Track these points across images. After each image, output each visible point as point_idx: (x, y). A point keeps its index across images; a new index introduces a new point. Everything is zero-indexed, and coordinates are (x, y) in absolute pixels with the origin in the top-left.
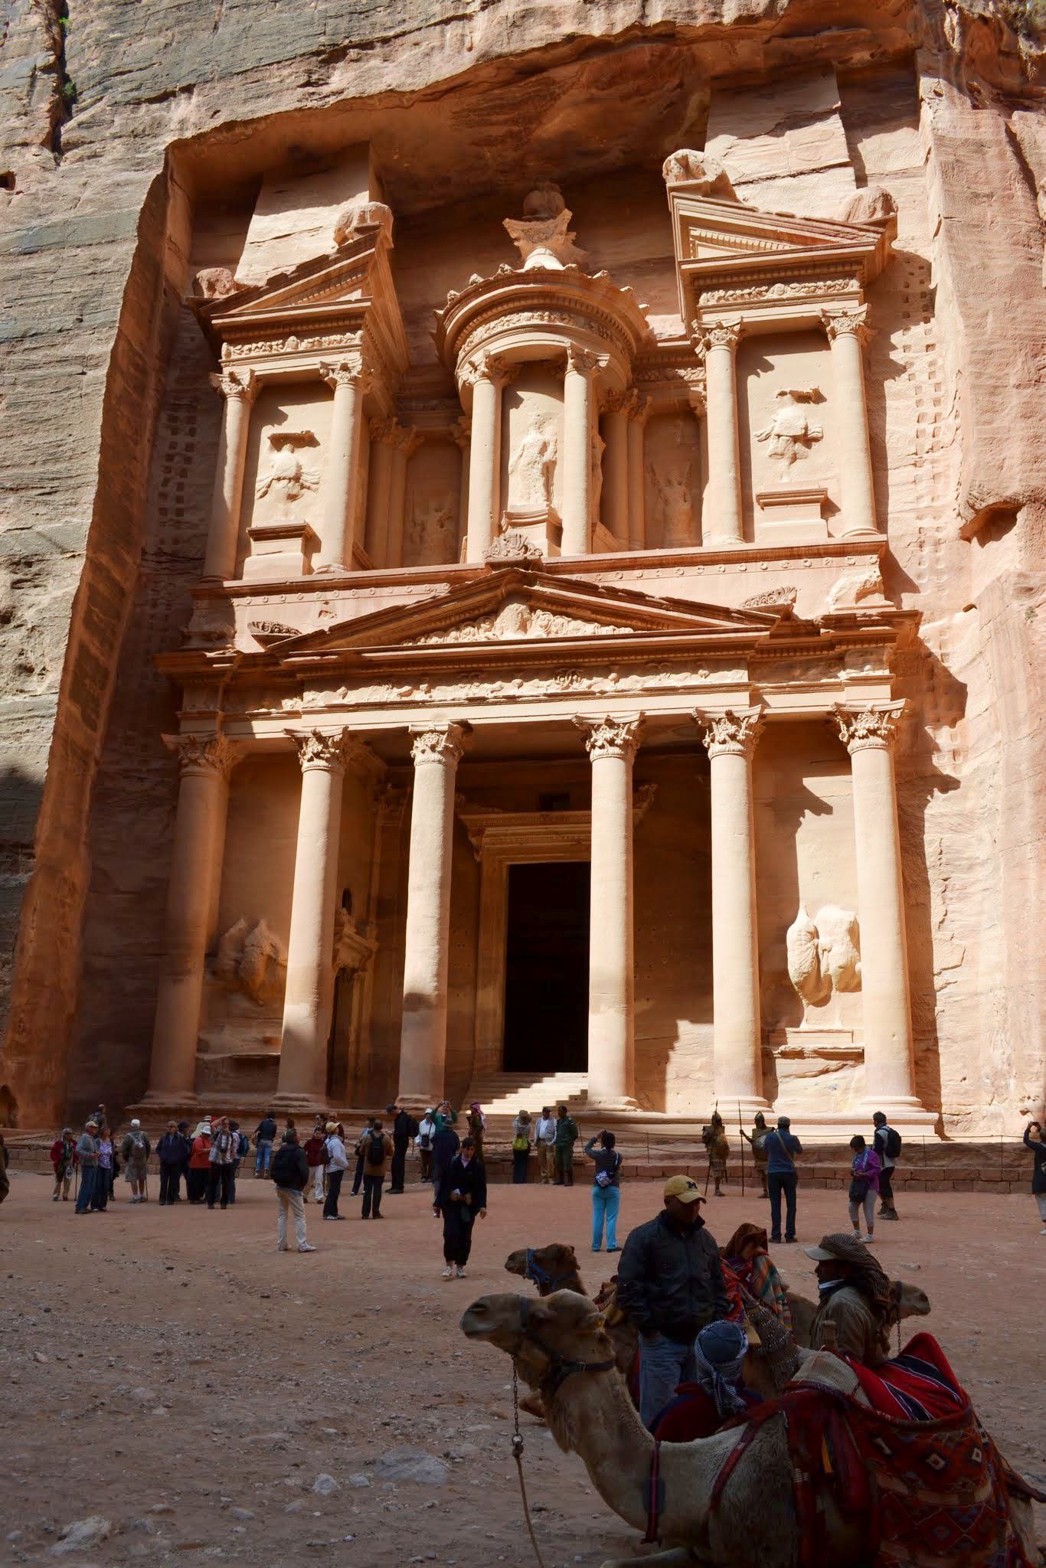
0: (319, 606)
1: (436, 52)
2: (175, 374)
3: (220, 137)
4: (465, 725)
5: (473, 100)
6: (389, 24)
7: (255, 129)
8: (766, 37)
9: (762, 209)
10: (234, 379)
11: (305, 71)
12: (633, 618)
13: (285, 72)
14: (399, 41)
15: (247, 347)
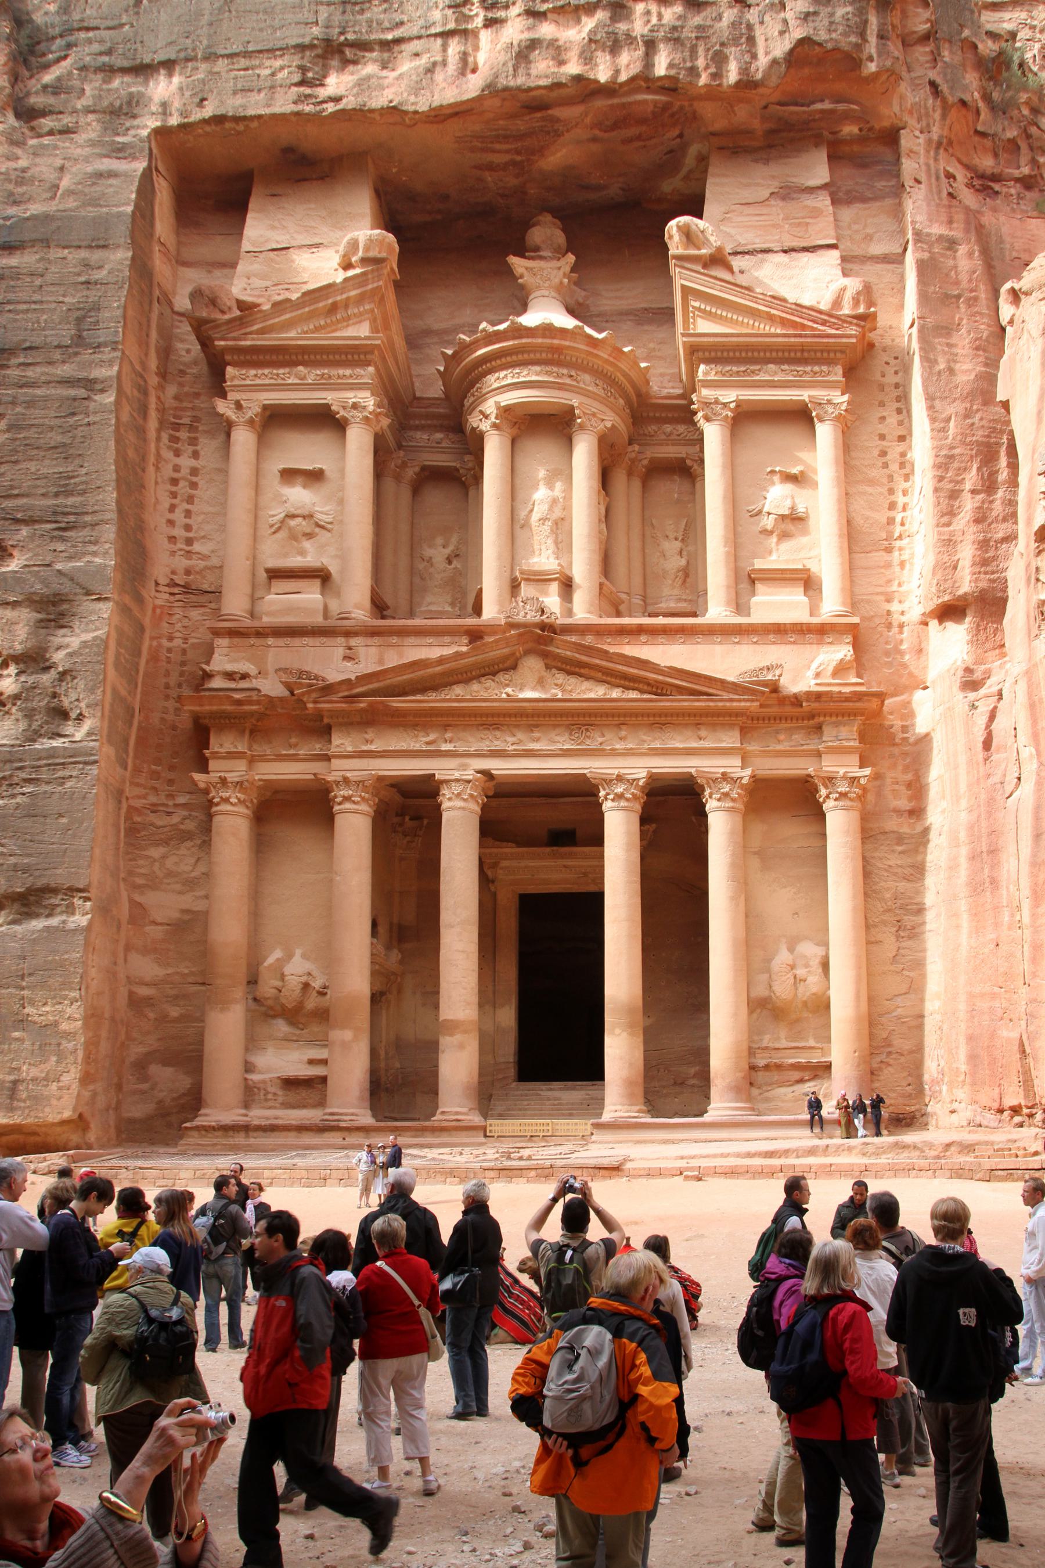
0: (340, 652)
1: (438, 69)
2: (172, 390)
3: (208, 129)
4: (487, 774)
5: (477, 127)
6: (387, 24)
7: (247, 126)
8: (763, 103)
9: (758, 290)
10: (238, 406)
11: (299, 67)
12: (640, 682)
13: (278, 63)
14: (396, 49)
15: (253, 372)
